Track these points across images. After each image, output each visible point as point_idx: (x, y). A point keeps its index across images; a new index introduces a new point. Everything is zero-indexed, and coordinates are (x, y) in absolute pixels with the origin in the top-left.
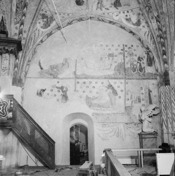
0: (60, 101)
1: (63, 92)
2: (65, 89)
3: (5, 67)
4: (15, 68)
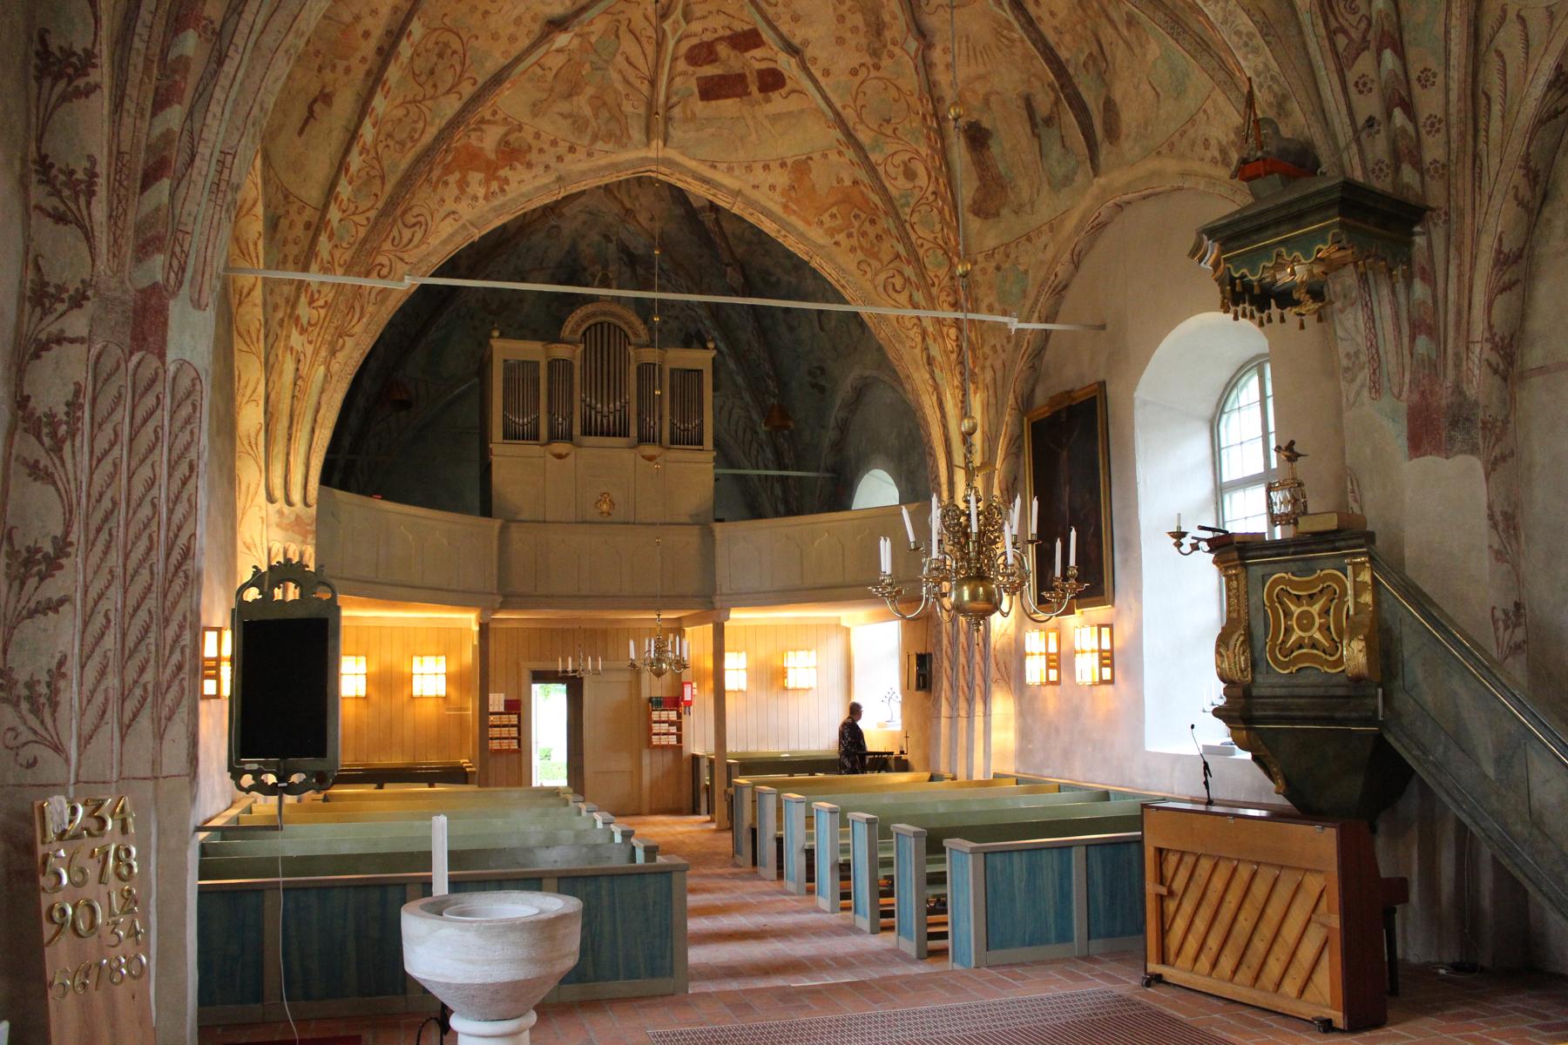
4: (1413, 339)
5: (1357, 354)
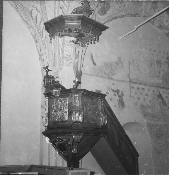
0: (117, 107)
1: (119, 96)
2: (120, 93)
3: (69, 54)
5: (70, 56)
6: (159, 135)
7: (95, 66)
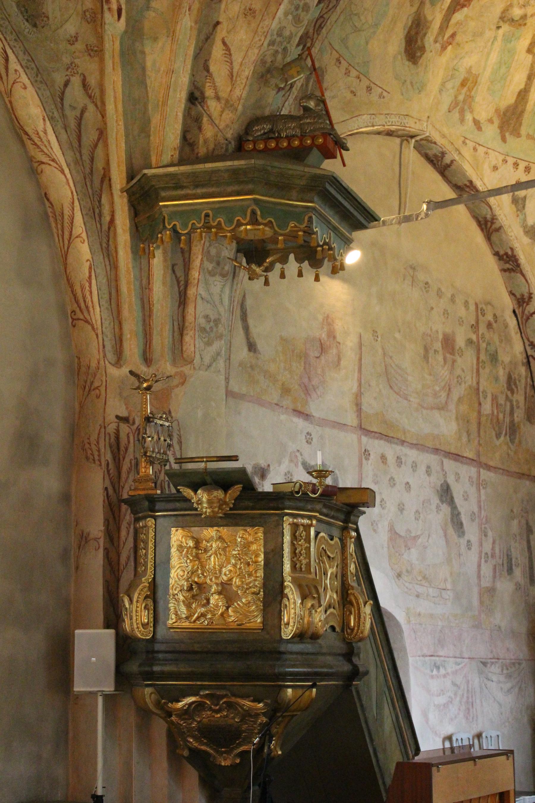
6: (437, 658)
7: (252, 354)
